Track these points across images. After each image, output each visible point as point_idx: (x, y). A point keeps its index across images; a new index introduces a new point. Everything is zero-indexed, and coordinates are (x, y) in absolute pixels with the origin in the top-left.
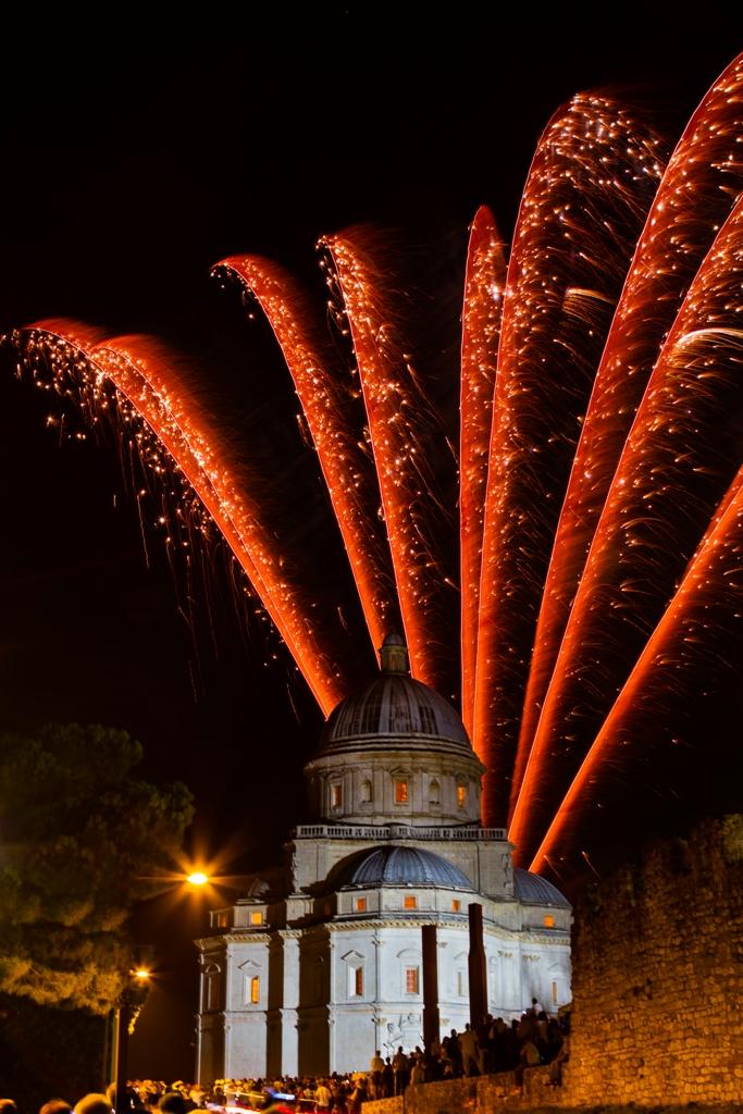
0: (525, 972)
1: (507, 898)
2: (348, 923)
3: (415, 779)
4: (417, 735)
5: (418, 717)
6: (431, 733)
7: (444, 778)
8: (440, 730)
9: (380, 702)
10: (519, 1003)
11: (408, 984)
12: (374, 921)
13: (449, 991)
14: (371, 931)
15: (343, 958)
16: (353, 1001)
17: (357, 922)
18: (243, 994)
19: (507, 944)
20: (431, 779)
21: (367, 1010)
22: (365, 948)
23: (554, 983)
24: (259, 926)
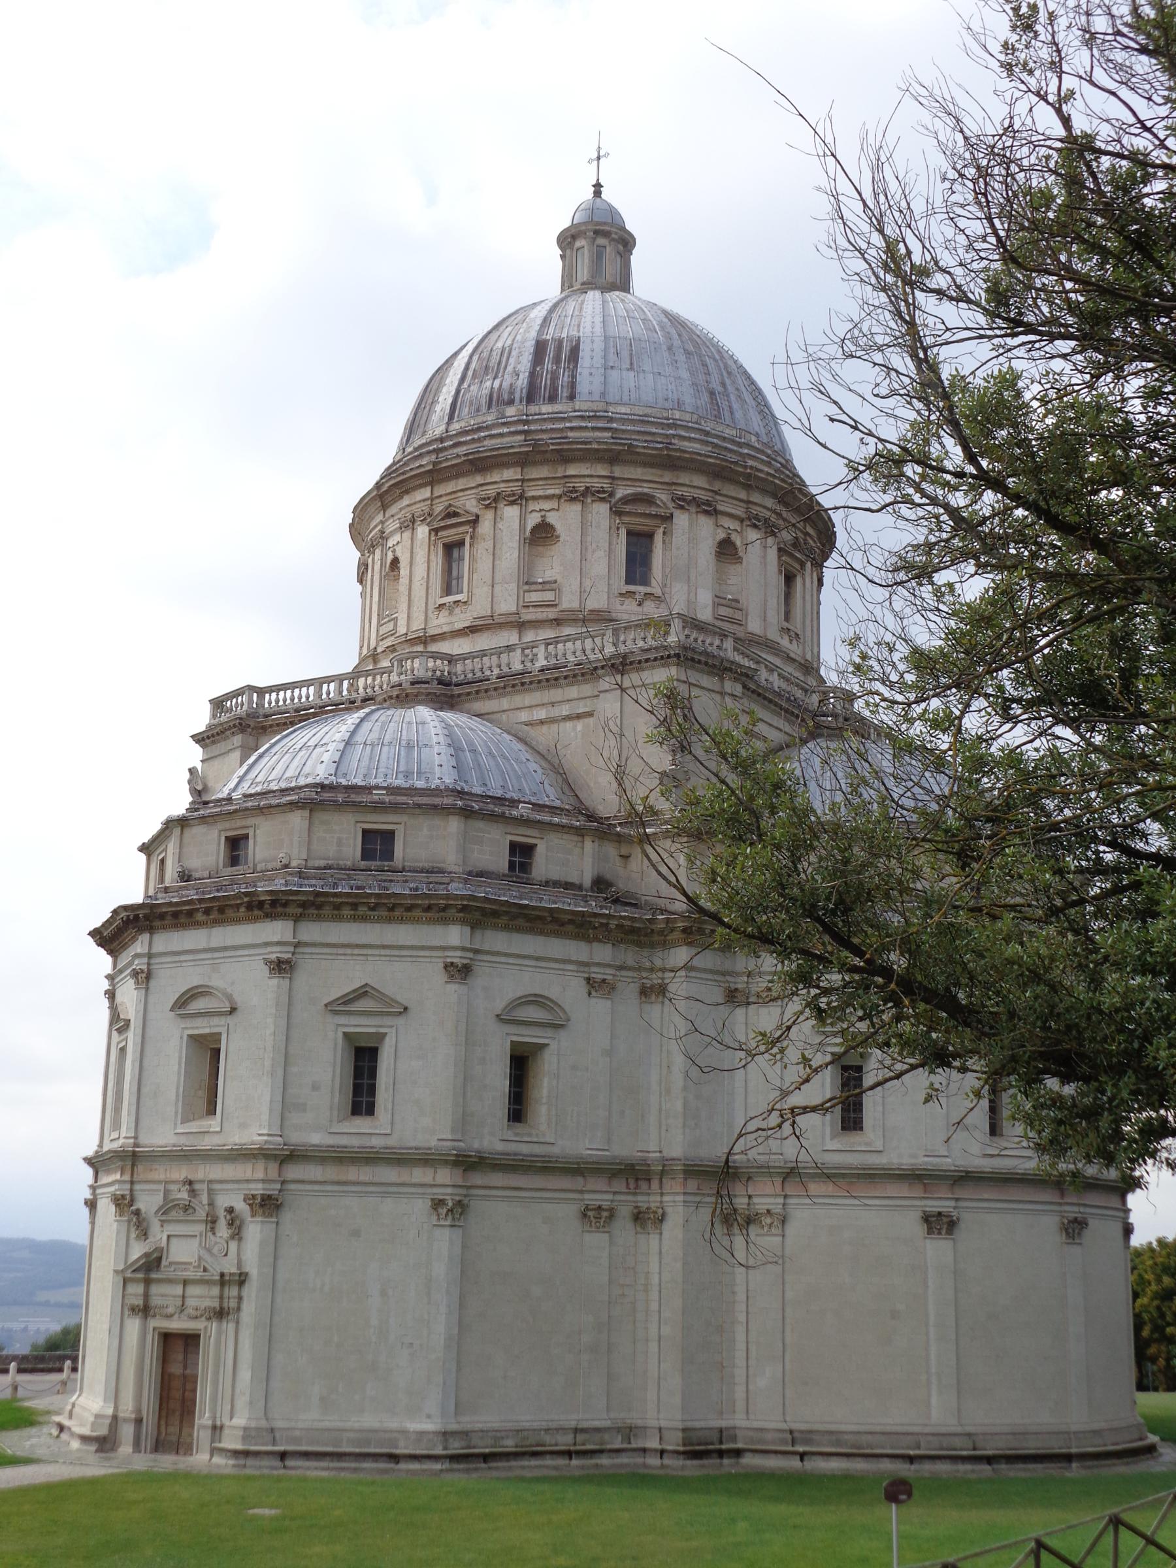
3: (485, 527)
6: (553, 398)
7: (573, 510)
8: (583, 386)
13: (286, 1106)
20: (533, 520)
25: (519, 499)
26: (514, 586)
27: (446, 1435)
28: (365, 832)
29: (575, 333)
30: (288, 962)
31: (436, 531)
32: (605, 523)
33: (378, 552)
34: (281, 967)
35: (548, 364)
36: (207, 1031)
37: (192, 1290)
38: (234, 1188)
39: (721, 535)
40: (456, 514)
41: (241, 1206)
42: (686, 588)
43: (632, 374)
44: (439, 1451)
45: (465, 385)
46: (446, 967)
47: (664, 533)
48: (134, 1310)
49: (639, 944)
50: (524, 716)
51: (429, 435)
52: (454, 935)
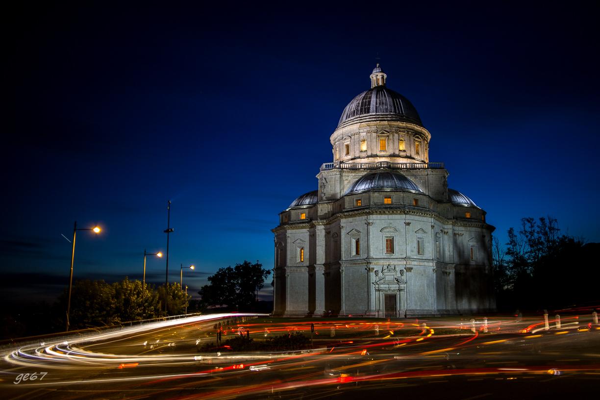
0: (455, 243)
1: (445, 201)
2: (351, 213)
3: (391, 137)
4: (392, 113)
5: (392, 104)
9: (370, 98)
10: (452, 259)
11: (387, 248)
12: (366, 210)
14: (364, 217)
15: (348, 234)
16: (354, 258)
17: (356, 212)
18: (296, 257)
19: (446, 227)
21: (362, 263)
22: (362, 227)
23: (472, 249)
24: (304, 220)
26: (398, 151)
27: (439, 311)
30: (410, 223)
32: (413, 140)
33: (356, 136)
34: (408, 224)
36: (390, 236)
37: (393, 286)
38: (401, 265)
40: (384, 133)
41: (405, 270)
44: (438, 313)
45: (378, 105)
48: (379, 290)
49: (443, 223)
51: (371, 114)
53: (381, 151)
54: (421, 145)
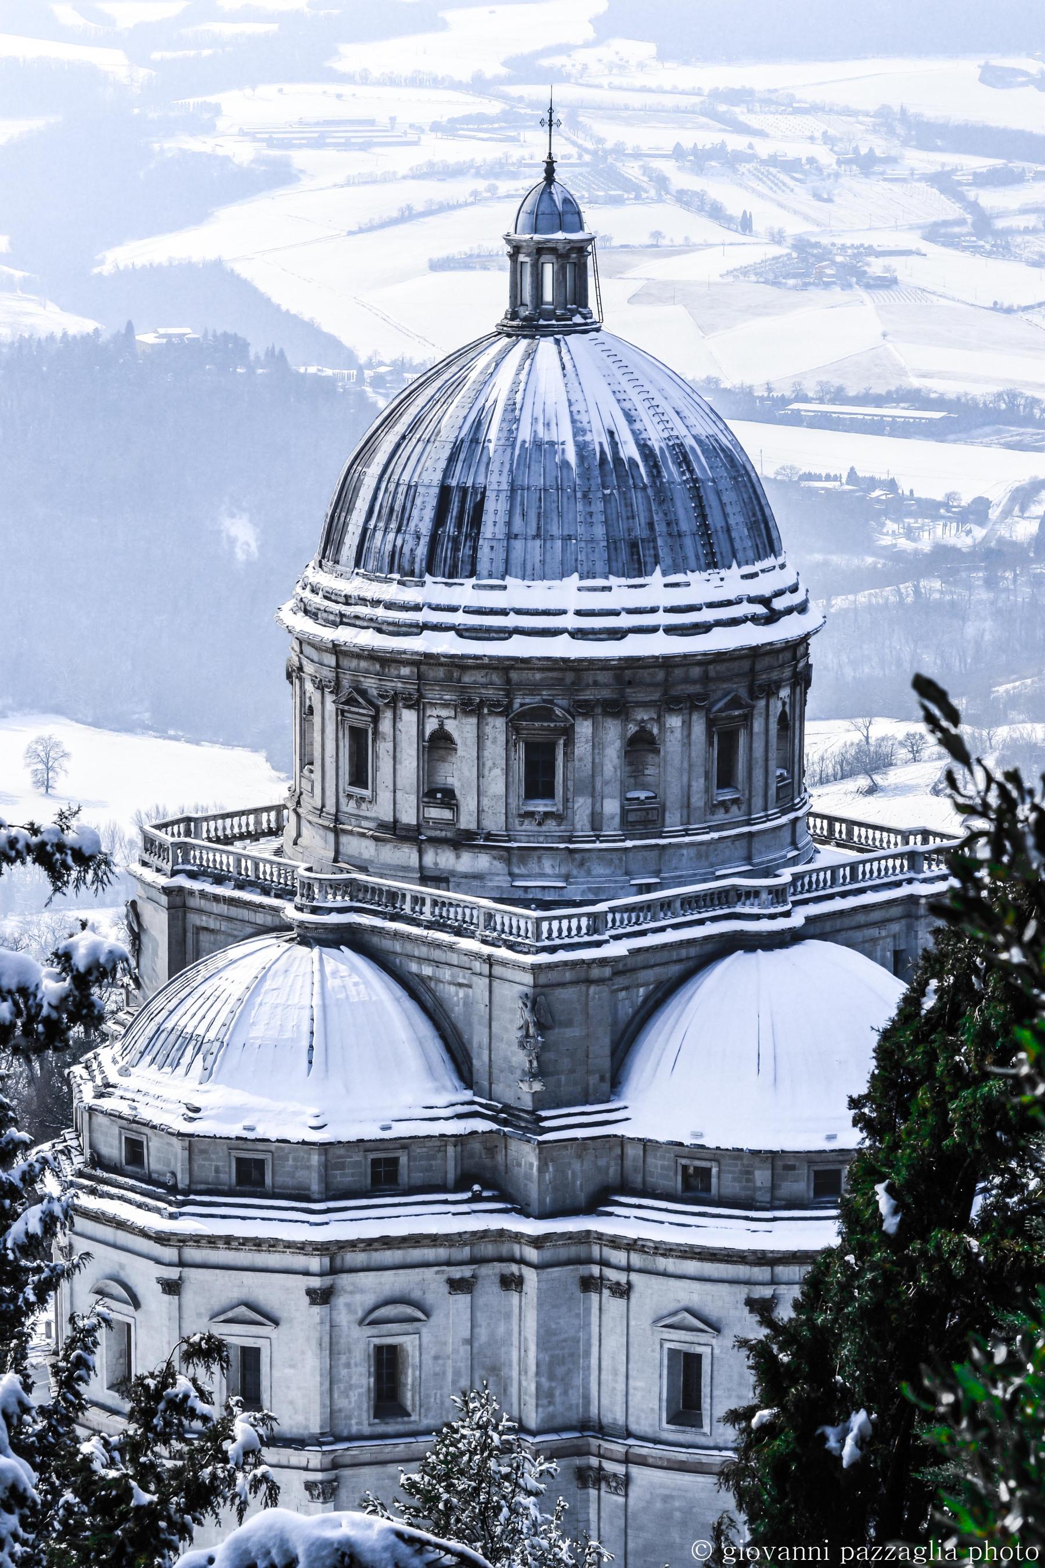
3: (386, 725)
20: (431, 725)
25: (417, 703)
26: (413, 798)
28: (240, 1161)
29: (481, 480)
31: (343, 712)
32: (502, 738)
35: (450, 528)
39: (632, 728)
42: (589, 801)
43: (538, 543)
45: (372, 524)
46: (310, 1292)
47: (565, 745)
50: (414, 967)
52: (315, 1263)
53: (350, 796)
54: (570, 743)
